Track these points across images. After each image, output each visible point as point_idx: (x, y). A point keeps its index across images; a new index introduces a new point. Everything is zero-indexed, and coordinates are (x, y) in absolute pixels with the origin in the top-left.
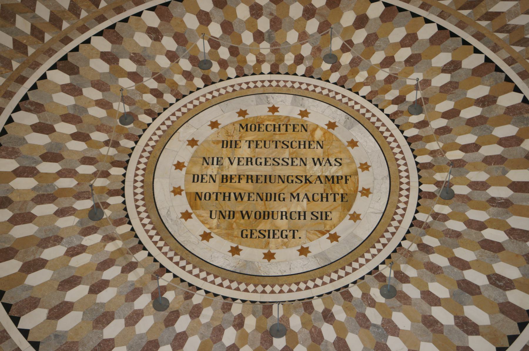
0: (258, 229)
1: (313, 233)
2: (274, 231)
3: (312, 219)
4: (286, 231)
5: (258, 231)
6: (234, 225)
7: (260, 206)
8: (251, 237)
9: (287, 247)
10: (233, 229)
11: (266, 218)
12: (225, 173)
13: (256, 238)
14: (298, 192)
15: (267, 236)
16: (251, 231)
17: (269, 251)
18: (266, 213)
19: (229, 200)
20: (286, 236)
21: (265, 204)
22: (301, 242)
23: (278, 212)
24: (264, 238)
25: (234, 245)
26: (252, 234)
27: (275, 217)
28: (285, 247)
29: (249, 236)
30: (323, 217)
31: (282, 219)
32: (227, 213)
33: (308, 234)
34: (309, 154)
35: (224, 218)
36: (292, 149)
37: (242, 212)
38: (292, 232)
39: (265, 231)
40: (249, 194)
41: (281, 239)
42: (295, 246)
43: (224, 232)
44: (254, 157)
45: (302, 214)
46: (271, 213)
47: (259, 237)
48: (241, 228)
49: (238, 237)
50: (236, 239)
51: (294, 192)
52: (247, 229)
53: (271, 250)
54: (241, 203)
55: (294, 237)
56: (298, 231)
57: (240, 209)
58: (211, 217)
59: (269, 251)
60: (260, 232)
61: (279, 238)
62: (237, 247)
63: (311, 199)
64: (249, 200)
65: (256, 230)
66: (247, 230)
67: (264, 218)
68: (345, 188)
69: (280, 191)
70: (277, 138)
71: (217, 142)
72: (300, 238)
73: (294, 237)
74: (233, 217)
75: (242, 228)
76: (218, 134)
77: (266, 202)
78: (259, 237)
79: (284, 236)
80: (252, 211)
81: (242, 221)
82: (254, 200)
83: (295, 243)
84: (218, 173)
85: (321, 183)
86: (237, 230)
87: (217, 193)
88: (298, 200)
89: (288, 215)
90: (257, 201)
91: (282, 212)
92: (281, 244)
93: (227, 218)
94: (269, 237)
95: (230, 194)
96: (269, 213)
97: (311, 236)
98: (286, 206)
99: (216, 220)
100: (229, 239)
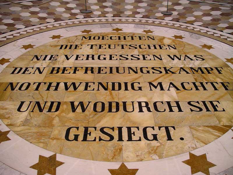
0: (99, 126)
1: (203, 130)
2: (129, 129)
3: (192, 110)
4: (153, 128)
5: (98, 129)
6: (56, 121)
7: (104, 96)
8: (85, 139)
9: (160, 157)
10: (51, 126)
11: (114, 110)
12: (57, 66)
13: (95, 140)
14: (159, 81)
15: (116, 137)
16: (86, 129)
17: (123, 166)
18: (114, 105)
19: (56, 89)
20: (155, 137)
21: (111, 94)
22: (187, 147)
23: (133, 102)
24: (110, 140)
25: (47, 154)
26: (86, 133)
27: (129, 108)
28: (155, 157)
29: (81, 138)
30: (209, 108)
31: (141, 110)
32: (49, 104)
33: (194, 132)
34: (163, 53)
35: (41, 110)
36: (141, 49)
37: (72, 103)
38: (163, 129)
39: (113, 129)
40: (87, 84)
41: (144, 141)
42: (177, 154)
43: (34, 130)
44: (97, 54)
45: (173, 104)
46: (121, 104)
47: (100, 139)
48: (66, 124)
49: (58, 139)
50: (55, 141)
51: (154, 81)
52: (79, 125)
53: (126, 164)
54: (75, 92)
55: (169, 138)
56: (174, 127)
57: (71, 99)
58: (19, 110)
59: (123, 166)
60: (102, 130)
61: (140, 140)
62: (53, 157)
63: (180, 87)
64: (86, 89)
65: (95, 128)
66: (78, 128)
67: (110, 110)
68: (222, 77)
69: (133, 81)
70: (123, 43)
71: (56, 46)
72: (182, 139)
73: (169, 138)
74: (57, 110)
75: (69, 125)
76: (58, 41)
77: (113, 91)
78: (100, 139)
79: (150, 137)
80: (89, 102)
81: (71, 115)
82: (93, 90)
83: (174, 148)
84: (47, 66)
85: (187, 73)
86: (59, 128)
87: (40, 84)
88: (162, 89)
89: (151, 106)
90: (98, 90)
91: (140, 103)
92: (146, 151)
93: (45, 111)
94: (120, 139)
95: (58, 84)
96: (117, 104)
97: (203, 135)
98: (145, 96)
99: (26, 114)
100: (41, 142)
